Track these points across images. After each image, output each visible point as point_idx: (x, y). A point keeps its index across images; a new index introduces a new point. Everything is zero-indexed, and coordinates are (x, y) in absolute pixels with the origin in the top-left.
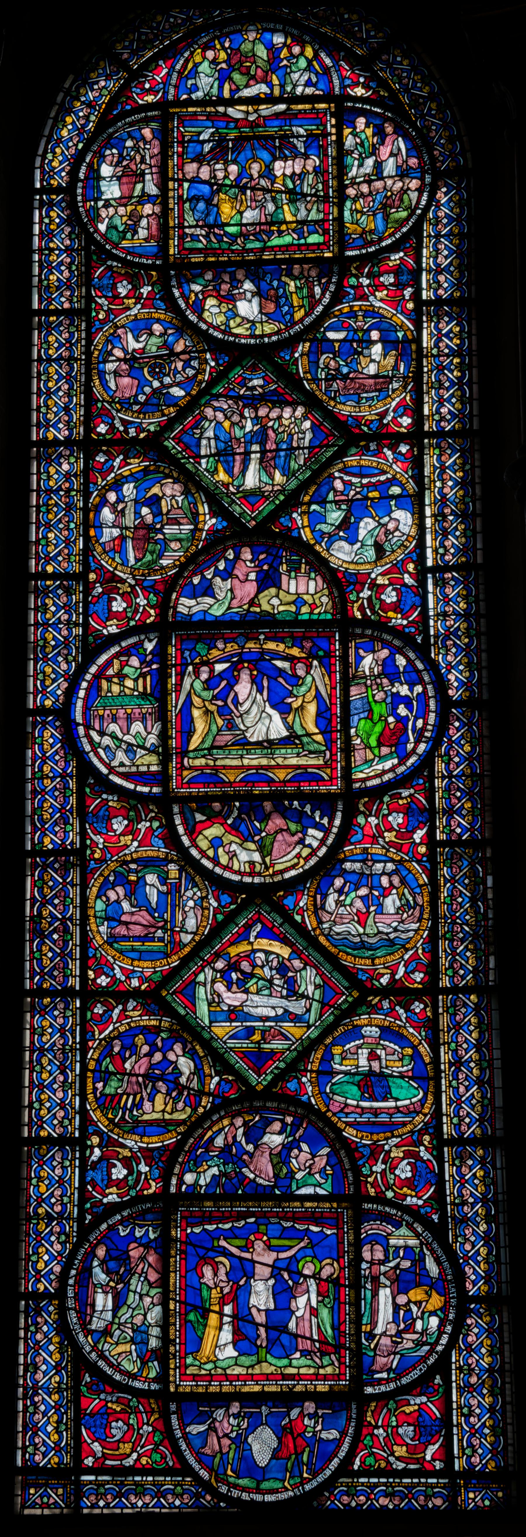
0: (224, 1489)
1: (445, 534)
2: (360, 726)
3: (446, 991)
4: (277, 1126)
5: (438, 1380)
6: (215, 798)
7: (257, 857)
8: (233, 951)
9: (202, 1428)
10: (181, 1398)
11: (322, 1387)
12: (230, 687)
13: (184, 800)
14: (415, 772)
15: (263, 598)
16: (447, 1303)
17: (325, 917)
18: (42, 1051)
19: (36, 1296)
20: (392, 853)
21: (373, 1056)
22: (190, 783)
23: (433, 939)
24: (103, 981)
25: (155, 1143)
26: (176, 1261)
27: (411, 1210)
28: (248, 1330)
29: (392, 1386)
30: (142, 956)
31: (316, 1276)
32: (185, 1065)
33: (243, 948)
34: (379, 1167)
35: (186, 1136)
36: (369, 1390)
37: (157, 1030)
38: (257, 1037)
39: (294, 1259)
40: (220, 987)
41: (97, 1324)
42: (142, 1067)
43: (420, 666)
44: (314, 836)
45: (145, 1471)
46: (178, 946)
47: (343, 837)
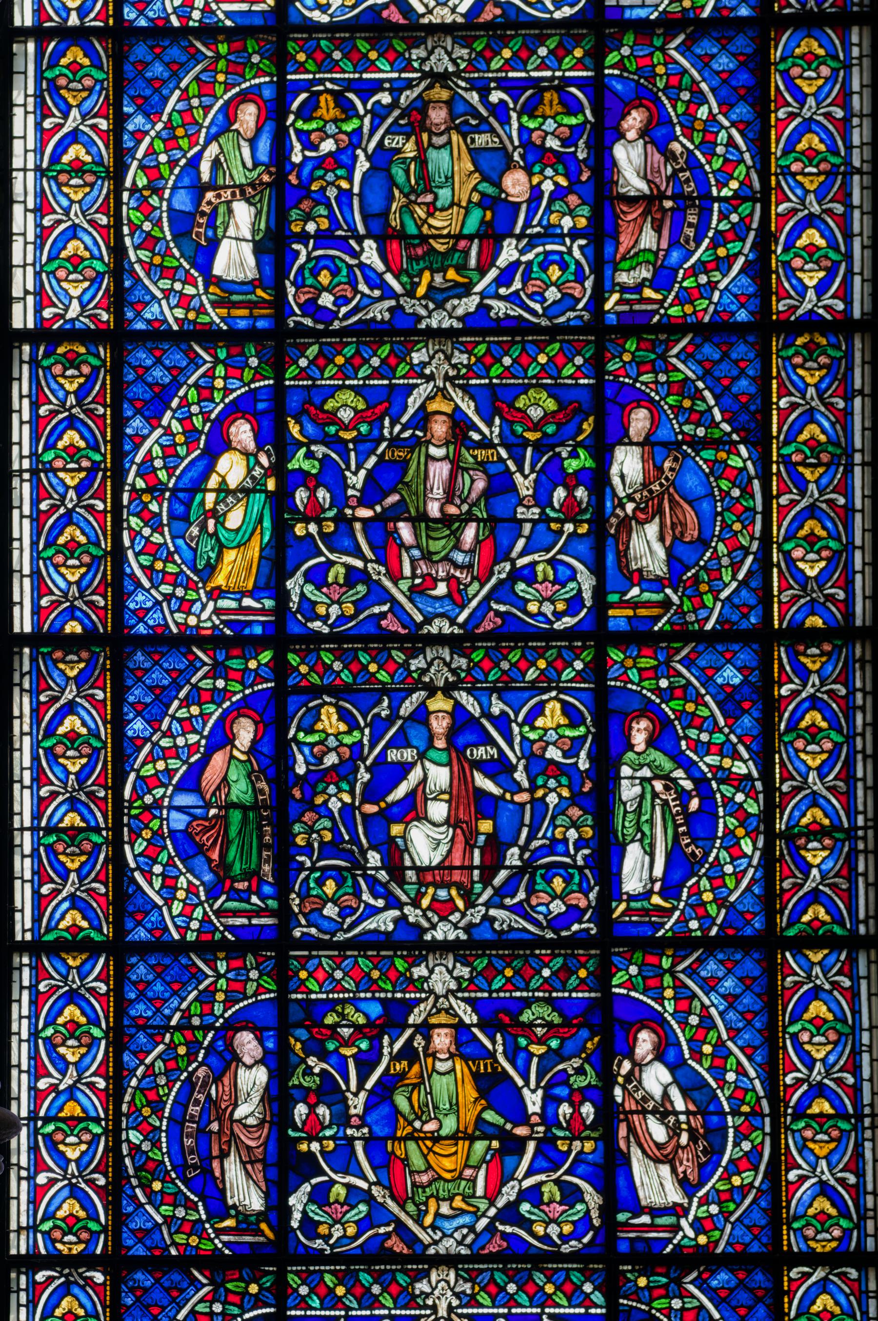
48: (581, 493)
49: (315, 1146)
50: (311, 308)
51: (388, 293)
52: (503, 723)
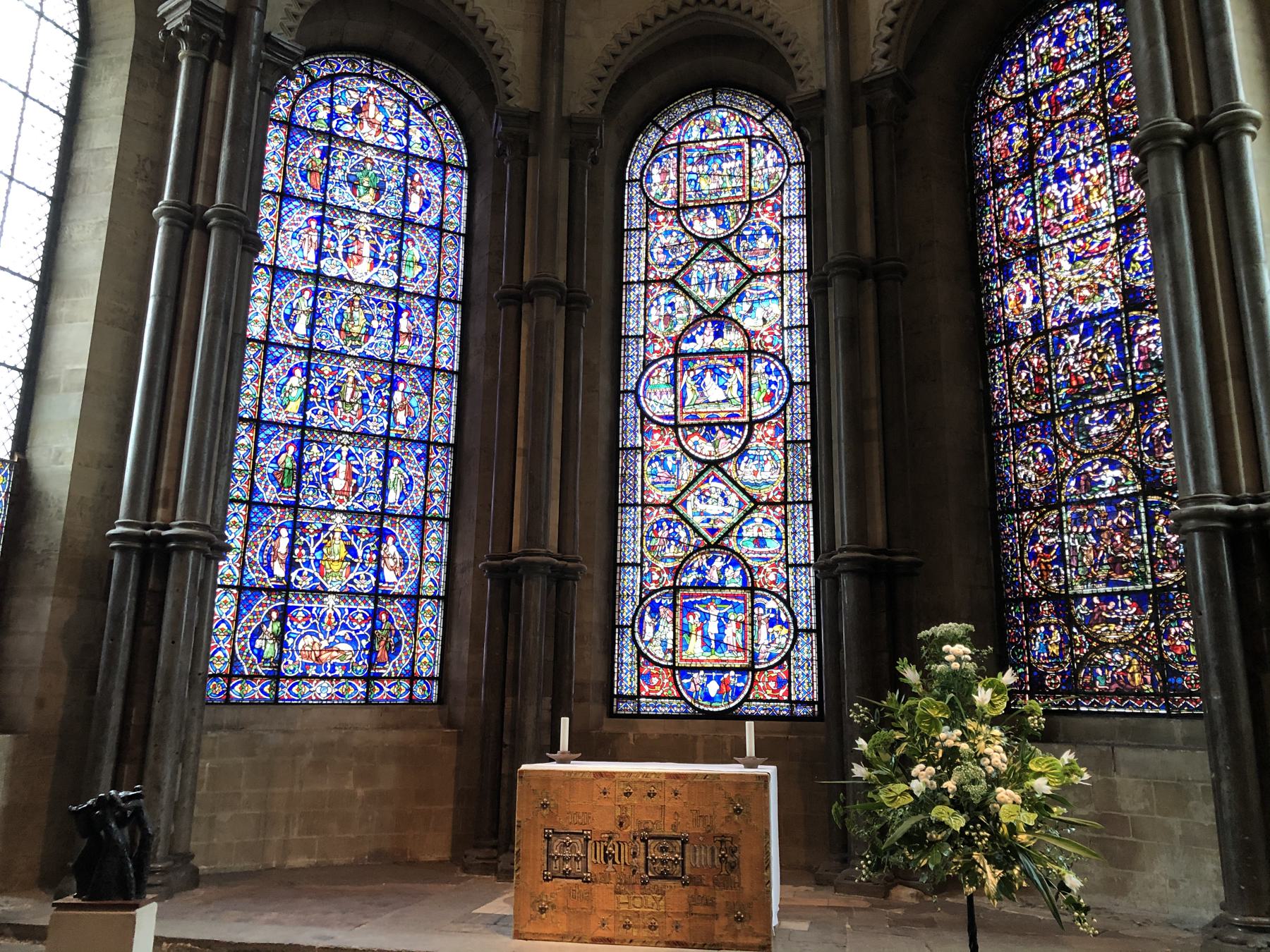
0: (697, 705)
1: (792, 313)
2: (756, 394)
3: (790, 503)
4: (720, 559)
5: (785, 663)
6: (696, 425)
7: (712, 449)
8: (702, 487)
9: (689, 680)
10: (680, 668)
11: (738, 665)
12: (702, 379)
13: (683, 426)
14: (779, 412)
15: (716, 342)
16: (789, 632)
17: (739, 472)
18: (625, 528)
19: (623, 627)
20: (769, 447)
21: (760, 530)
22: (687, 418)
23: (785, 481)
24: (650, 500)
25: (670, 564)
26: (678, 614)
27: (773, 593)
28: (707, 642)
29: (766, 665)
30: (666, 489)
31: (735, 620)
32: (683, 534)
33: (706, 486)
34: (761, 575)
35: (683, 562)
36: (757, 667)
37: (671, 520)
38: (712, 522)
39: (726, 613)
40: (697, 501)
41: (647, 638)
42: (665, 535)
43: (780, 368)
44: (736, 439)
45: (665, 698)
46: (679, 486)
47: (748, 440)
48: (386, 401)
49: (300, 561)
50: (319, 344)
51: (339, 344)
52: (361, 456)
